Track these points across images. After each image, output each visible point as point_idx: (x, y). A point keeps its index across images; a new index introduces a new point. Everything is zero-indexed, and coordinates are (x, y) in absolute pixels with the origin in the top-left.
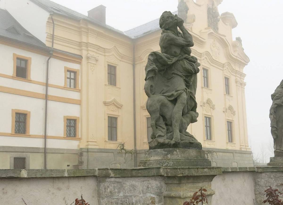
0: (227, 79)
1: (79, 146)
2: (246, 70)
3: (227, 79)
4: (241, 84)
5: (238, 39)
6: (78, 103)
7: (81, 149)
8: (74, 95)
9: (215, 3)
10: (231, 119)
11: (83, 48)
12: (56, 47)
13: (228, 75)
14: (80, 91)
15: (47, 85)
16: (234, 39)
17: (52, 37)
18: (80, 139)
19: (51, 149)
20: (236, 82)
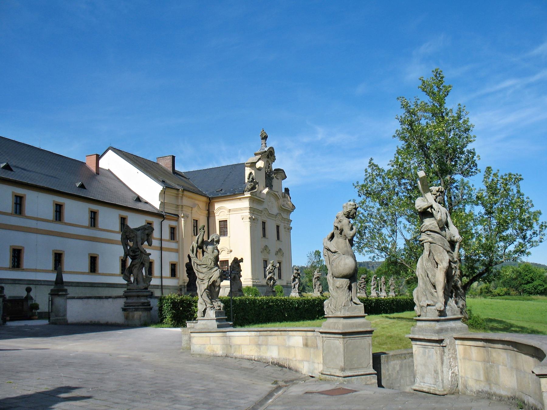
0: (278, 227)
1: (178, 283)
2: (292, 216)
3: (278, 227)
4: (288, 229)
5: (287, 190)
6: (177, 251)
7: (181, 286)
8: (173, 245)
9: (271, 163)
10: (280, 260)
11: (180, 209)
12: (166, 211)
13: (279, 223)
14: (177, 242)
15: (161, 240)
16: (283, 191)
17: (163, 204)
18: (178, 278)
19: (164, 286)
20: (285, 228)
